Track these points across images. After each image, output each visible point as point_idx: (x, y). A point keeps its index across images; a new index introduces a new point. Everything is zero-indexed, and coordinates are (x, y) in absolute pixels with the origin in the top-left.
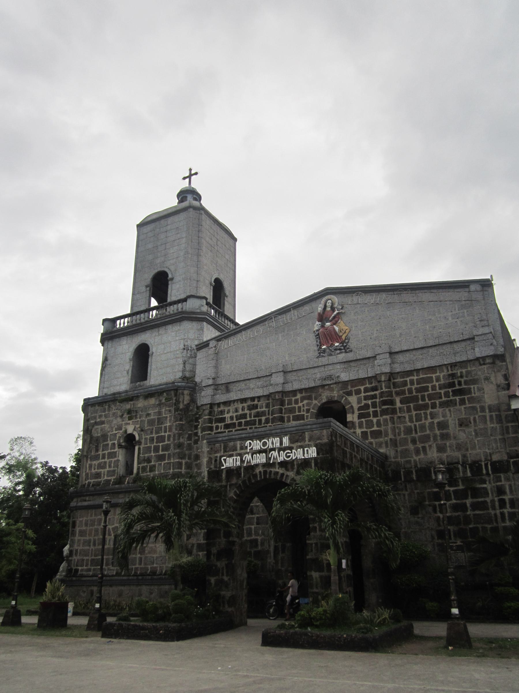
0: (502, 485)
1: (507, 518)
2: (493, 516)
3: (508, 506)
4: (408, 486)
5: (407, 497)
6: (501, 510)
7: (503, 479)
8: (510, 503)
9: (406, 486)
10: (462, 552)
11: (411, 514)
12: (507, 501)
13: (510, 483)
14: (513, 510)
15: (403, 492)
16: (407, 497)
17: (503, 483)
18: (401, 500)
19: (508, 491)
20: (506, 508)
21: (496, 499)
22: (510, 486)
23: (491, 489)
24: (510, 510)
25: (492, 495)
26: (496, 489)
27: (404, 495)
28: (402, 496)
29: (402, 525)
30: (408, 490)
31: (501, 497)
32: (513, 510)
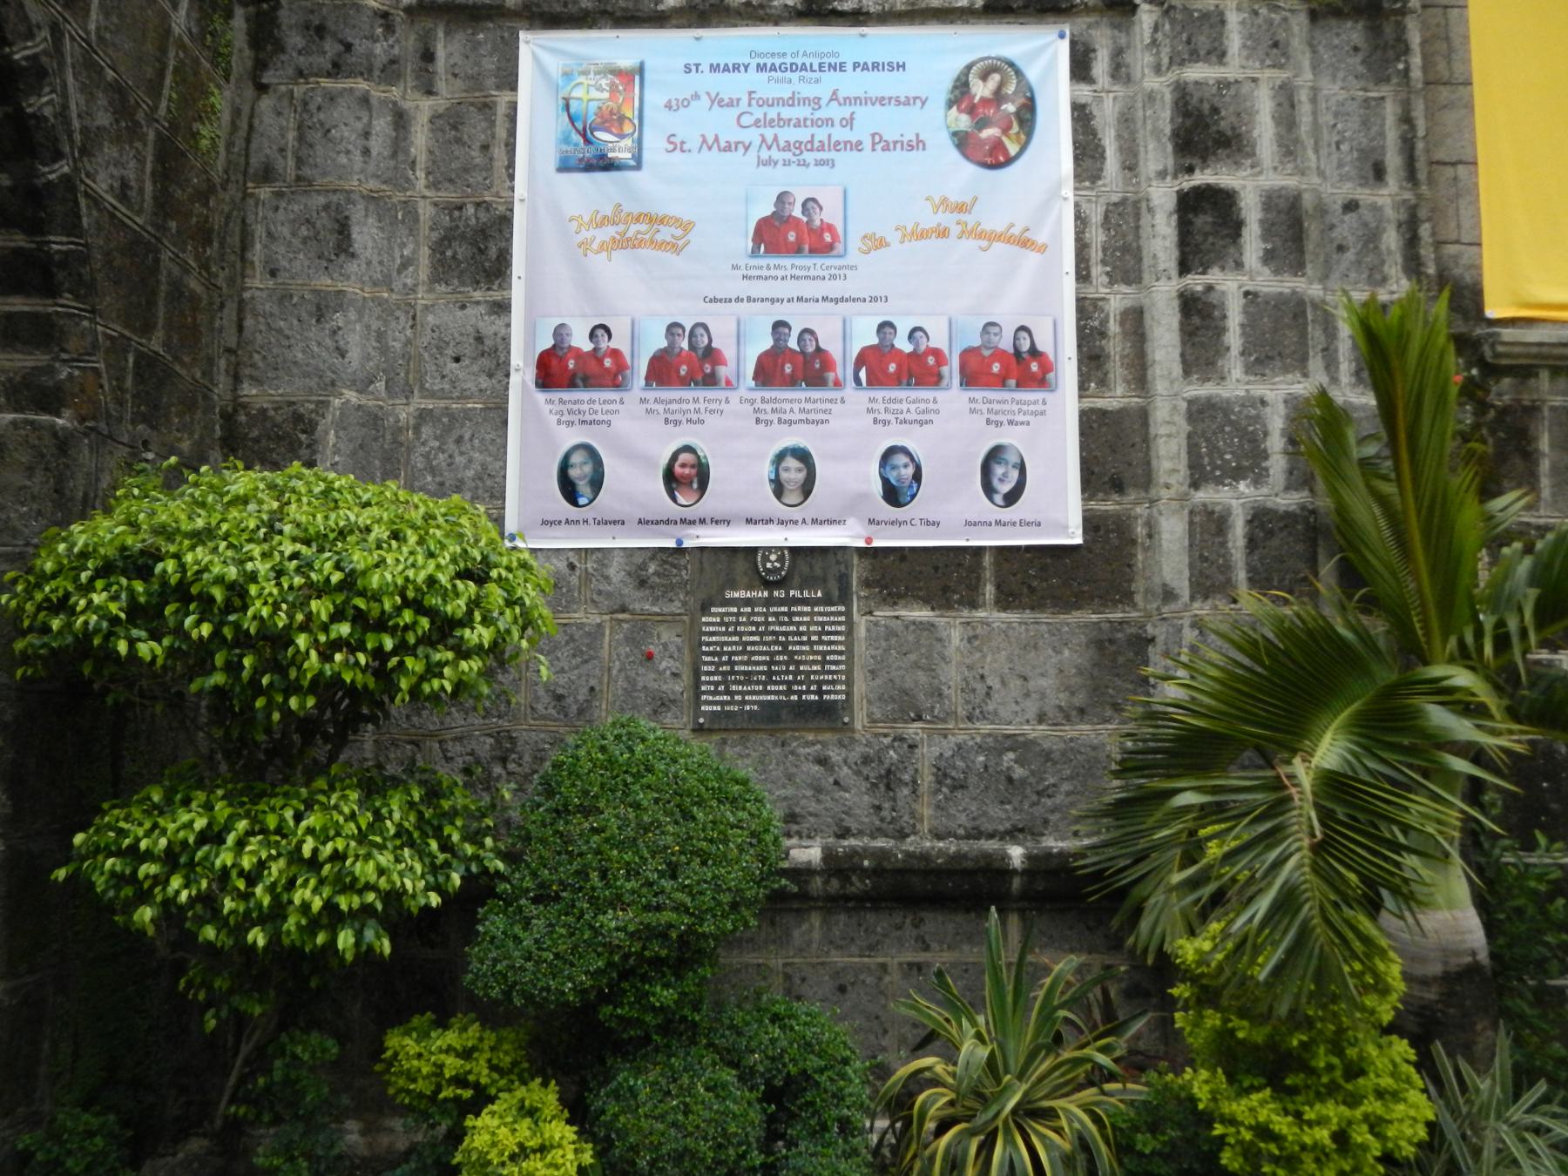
0: (1224, 84)
1: (1234, 338)
2: (1113, 327)
3: (1252, 243)
4: (441, 52)
5: (420, 139)
6: (1195, 282)
7: (1234, 41)
8: (1268, 231)
9: (428, 56)
10: (827, 601)
11: (435, 279)
12: (1251, 211)
13: (1284, 75)
14: (1288, 284)
15: (395, 92)
16: (420, 139)
17: (1232, 70)
18: (366, 152)
19: (1264, 131)
20: (1239, 265)
21: (1163, 196)
22: (1286, 97)
23: (1126, 120)
24: (1269, 283)
25: (1130, 166)
26: (1166, 114)
27: (401, 120)
28: (382, 125)
29: (343, 354)
30: (441, 85)
31: (1202, 178)
32: (1288, 284)
